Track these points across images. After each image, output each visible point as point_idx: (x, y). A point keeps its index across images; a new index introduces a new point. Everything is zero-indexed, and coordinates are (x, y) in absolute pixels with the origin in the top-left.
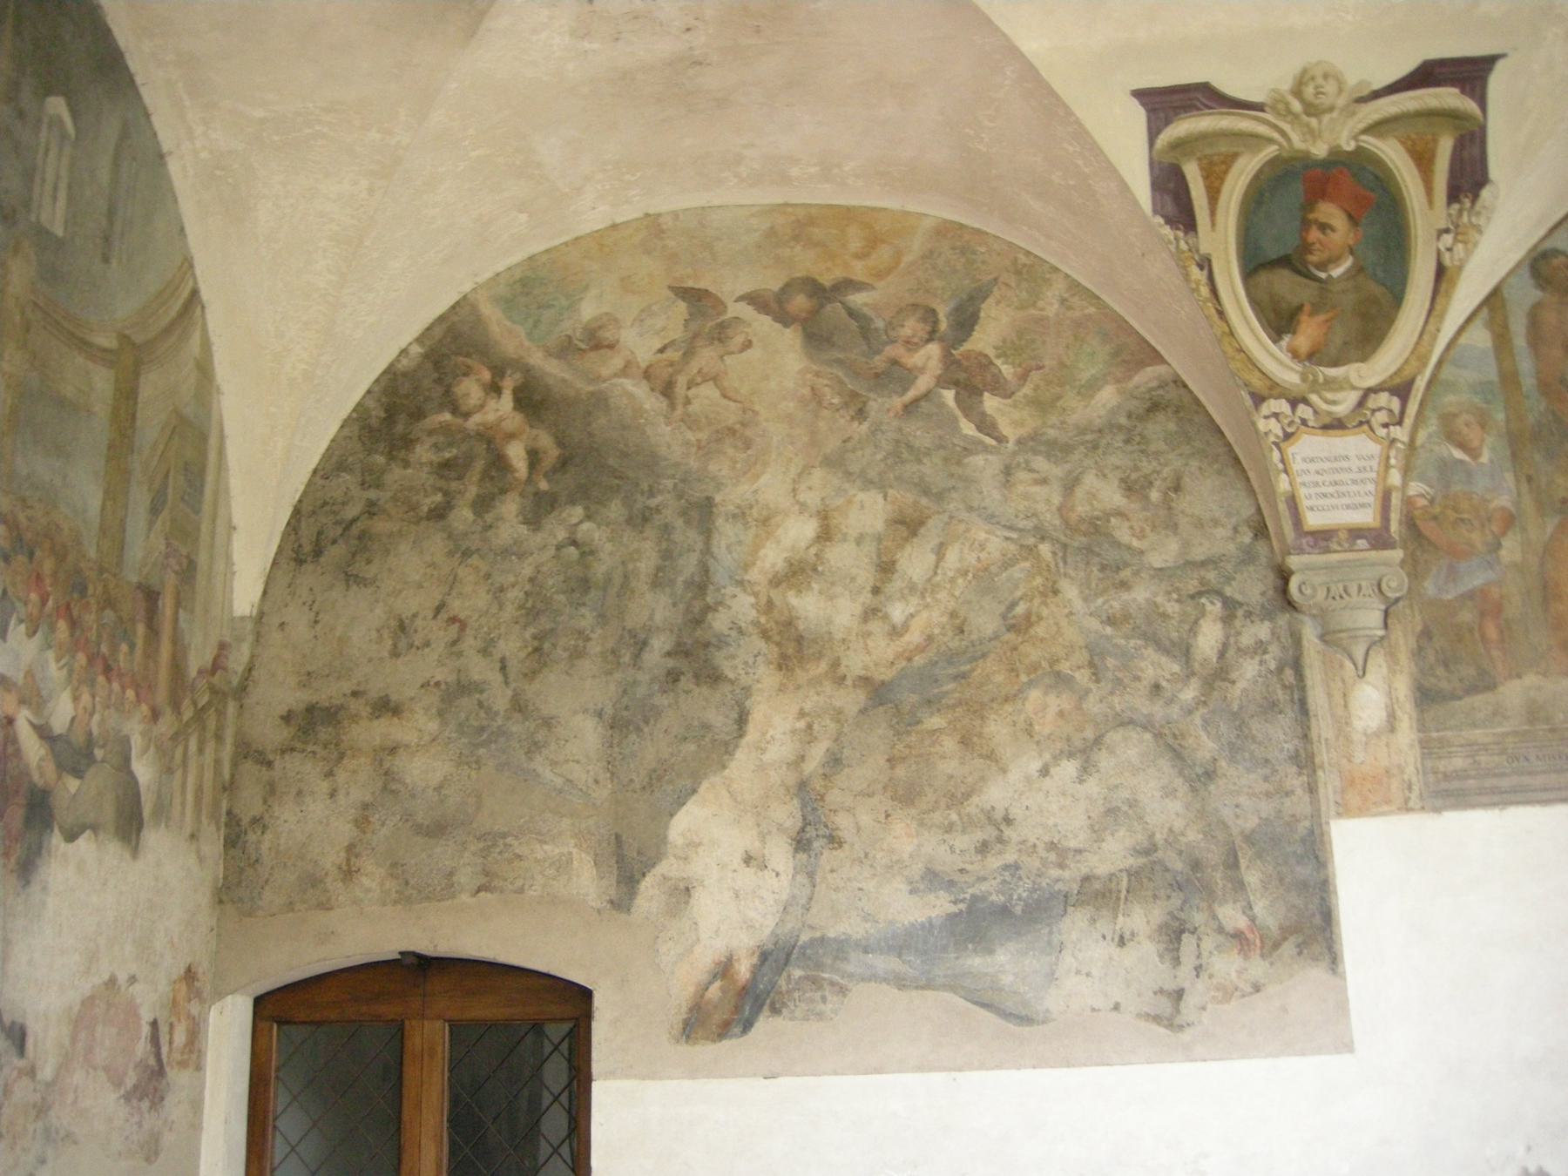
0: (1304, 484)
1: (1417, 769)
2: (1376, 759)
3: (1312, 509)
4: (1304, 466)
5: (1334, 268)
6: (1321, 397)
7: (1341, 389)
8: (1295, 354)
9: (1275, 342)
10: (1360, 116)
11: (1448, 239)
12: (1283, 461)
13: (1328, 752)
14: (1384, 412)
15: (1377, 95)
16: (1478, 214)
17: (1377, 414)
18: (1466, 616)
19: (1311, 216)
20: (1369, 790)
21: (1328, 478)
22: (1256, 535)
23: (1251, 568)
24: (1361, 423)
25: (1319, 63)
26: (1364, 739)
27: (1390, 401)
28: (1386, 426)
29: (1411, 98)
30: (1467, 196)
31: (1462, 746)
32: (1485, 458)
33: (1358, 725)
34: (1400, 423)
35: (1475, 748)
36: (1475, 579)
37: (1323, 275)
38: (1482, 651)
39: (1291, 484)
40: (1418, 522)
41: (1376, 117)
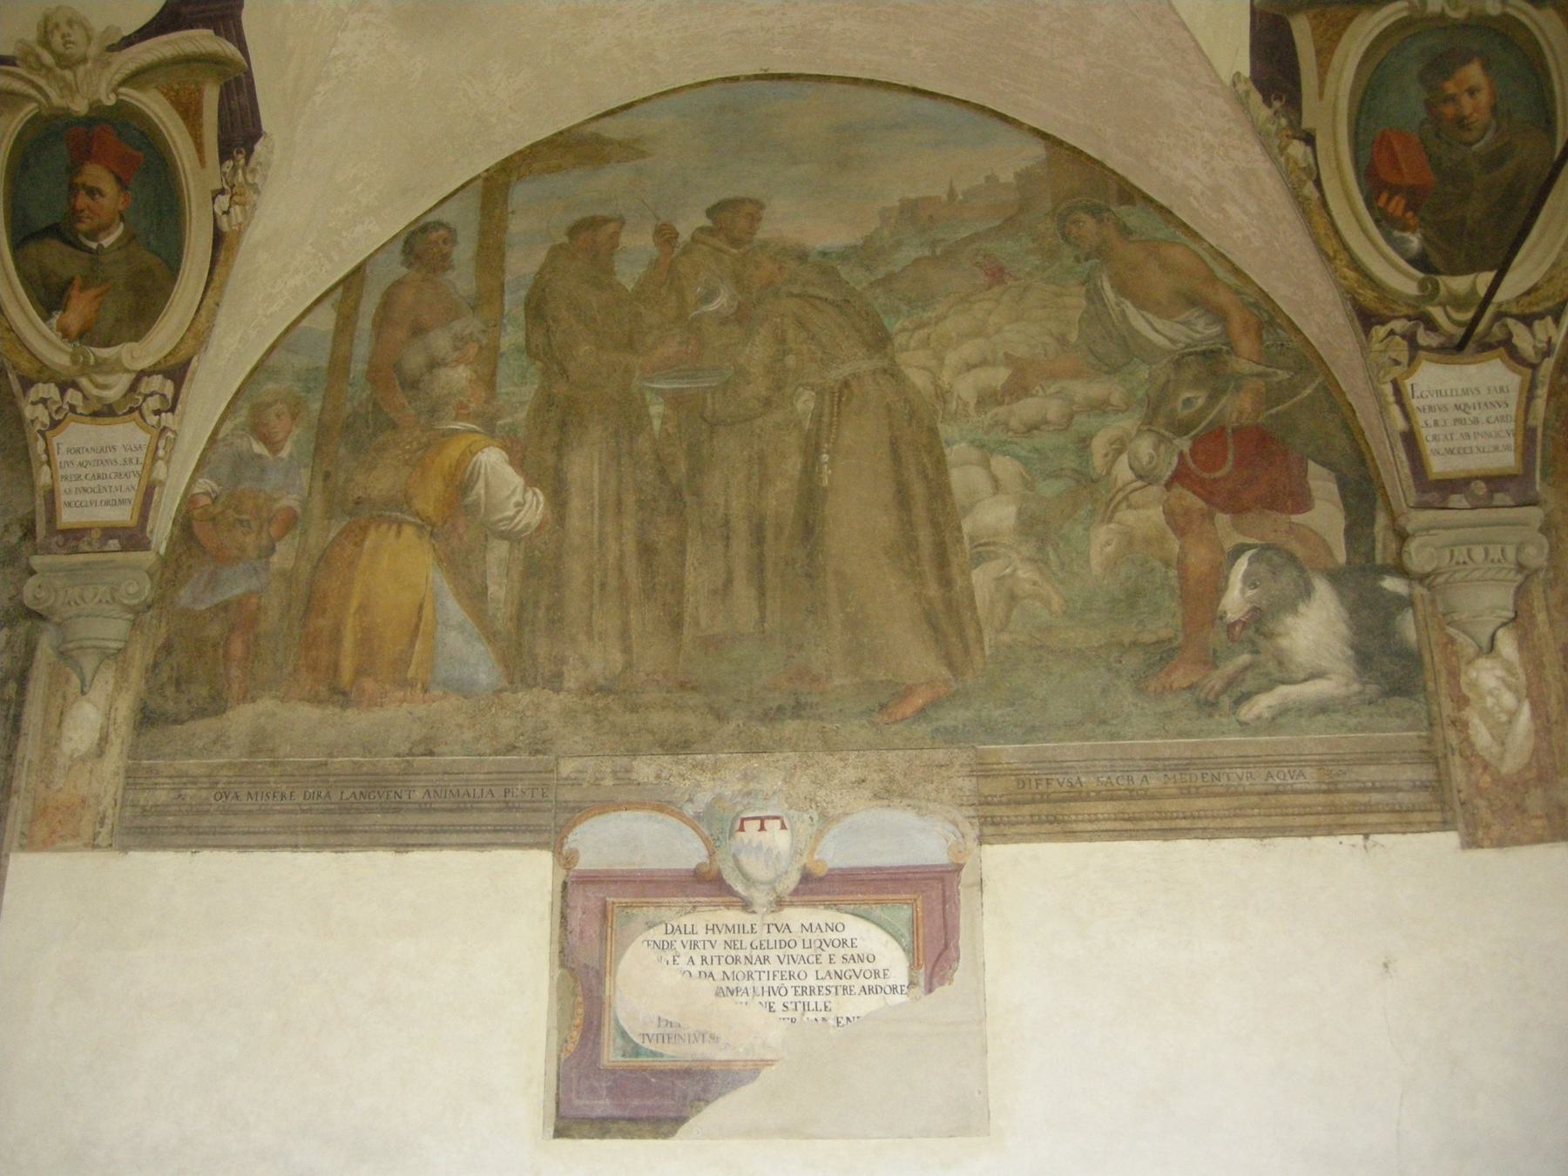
1: (115, 801)
2: (75, 787)
3: (70, 505)
4: (68, 457)
5: (105, 238)
6: (91, 381)
7: (112, 371)
8: (65, 334)
9: (45, 320)
10: (113, 68)
11: (223, 201)
12: (47, 451)
13: (28, 776)
14: (157, 397)
15: (128, 42)
16: (253, 171)
17: (149, 399)
18: (214, 630)
19: (79, 180)
20: (60, 822)
21: (90, 470)
22: (25, 535)
23: (8, 571)
24: (132, 410)
25: (58, 8)
28: (157, 412)
29: (166, 43)
30: (239, 152)
31: (171, 777)
32: (284, 454)
33: (67, 747)
34: (172, 410)
35: (184, 780)
36: (236, 586)
37: (94, 245)
38: (222, 671)
39: (52, 477)
40: (195, 524)
41: (132, 66)
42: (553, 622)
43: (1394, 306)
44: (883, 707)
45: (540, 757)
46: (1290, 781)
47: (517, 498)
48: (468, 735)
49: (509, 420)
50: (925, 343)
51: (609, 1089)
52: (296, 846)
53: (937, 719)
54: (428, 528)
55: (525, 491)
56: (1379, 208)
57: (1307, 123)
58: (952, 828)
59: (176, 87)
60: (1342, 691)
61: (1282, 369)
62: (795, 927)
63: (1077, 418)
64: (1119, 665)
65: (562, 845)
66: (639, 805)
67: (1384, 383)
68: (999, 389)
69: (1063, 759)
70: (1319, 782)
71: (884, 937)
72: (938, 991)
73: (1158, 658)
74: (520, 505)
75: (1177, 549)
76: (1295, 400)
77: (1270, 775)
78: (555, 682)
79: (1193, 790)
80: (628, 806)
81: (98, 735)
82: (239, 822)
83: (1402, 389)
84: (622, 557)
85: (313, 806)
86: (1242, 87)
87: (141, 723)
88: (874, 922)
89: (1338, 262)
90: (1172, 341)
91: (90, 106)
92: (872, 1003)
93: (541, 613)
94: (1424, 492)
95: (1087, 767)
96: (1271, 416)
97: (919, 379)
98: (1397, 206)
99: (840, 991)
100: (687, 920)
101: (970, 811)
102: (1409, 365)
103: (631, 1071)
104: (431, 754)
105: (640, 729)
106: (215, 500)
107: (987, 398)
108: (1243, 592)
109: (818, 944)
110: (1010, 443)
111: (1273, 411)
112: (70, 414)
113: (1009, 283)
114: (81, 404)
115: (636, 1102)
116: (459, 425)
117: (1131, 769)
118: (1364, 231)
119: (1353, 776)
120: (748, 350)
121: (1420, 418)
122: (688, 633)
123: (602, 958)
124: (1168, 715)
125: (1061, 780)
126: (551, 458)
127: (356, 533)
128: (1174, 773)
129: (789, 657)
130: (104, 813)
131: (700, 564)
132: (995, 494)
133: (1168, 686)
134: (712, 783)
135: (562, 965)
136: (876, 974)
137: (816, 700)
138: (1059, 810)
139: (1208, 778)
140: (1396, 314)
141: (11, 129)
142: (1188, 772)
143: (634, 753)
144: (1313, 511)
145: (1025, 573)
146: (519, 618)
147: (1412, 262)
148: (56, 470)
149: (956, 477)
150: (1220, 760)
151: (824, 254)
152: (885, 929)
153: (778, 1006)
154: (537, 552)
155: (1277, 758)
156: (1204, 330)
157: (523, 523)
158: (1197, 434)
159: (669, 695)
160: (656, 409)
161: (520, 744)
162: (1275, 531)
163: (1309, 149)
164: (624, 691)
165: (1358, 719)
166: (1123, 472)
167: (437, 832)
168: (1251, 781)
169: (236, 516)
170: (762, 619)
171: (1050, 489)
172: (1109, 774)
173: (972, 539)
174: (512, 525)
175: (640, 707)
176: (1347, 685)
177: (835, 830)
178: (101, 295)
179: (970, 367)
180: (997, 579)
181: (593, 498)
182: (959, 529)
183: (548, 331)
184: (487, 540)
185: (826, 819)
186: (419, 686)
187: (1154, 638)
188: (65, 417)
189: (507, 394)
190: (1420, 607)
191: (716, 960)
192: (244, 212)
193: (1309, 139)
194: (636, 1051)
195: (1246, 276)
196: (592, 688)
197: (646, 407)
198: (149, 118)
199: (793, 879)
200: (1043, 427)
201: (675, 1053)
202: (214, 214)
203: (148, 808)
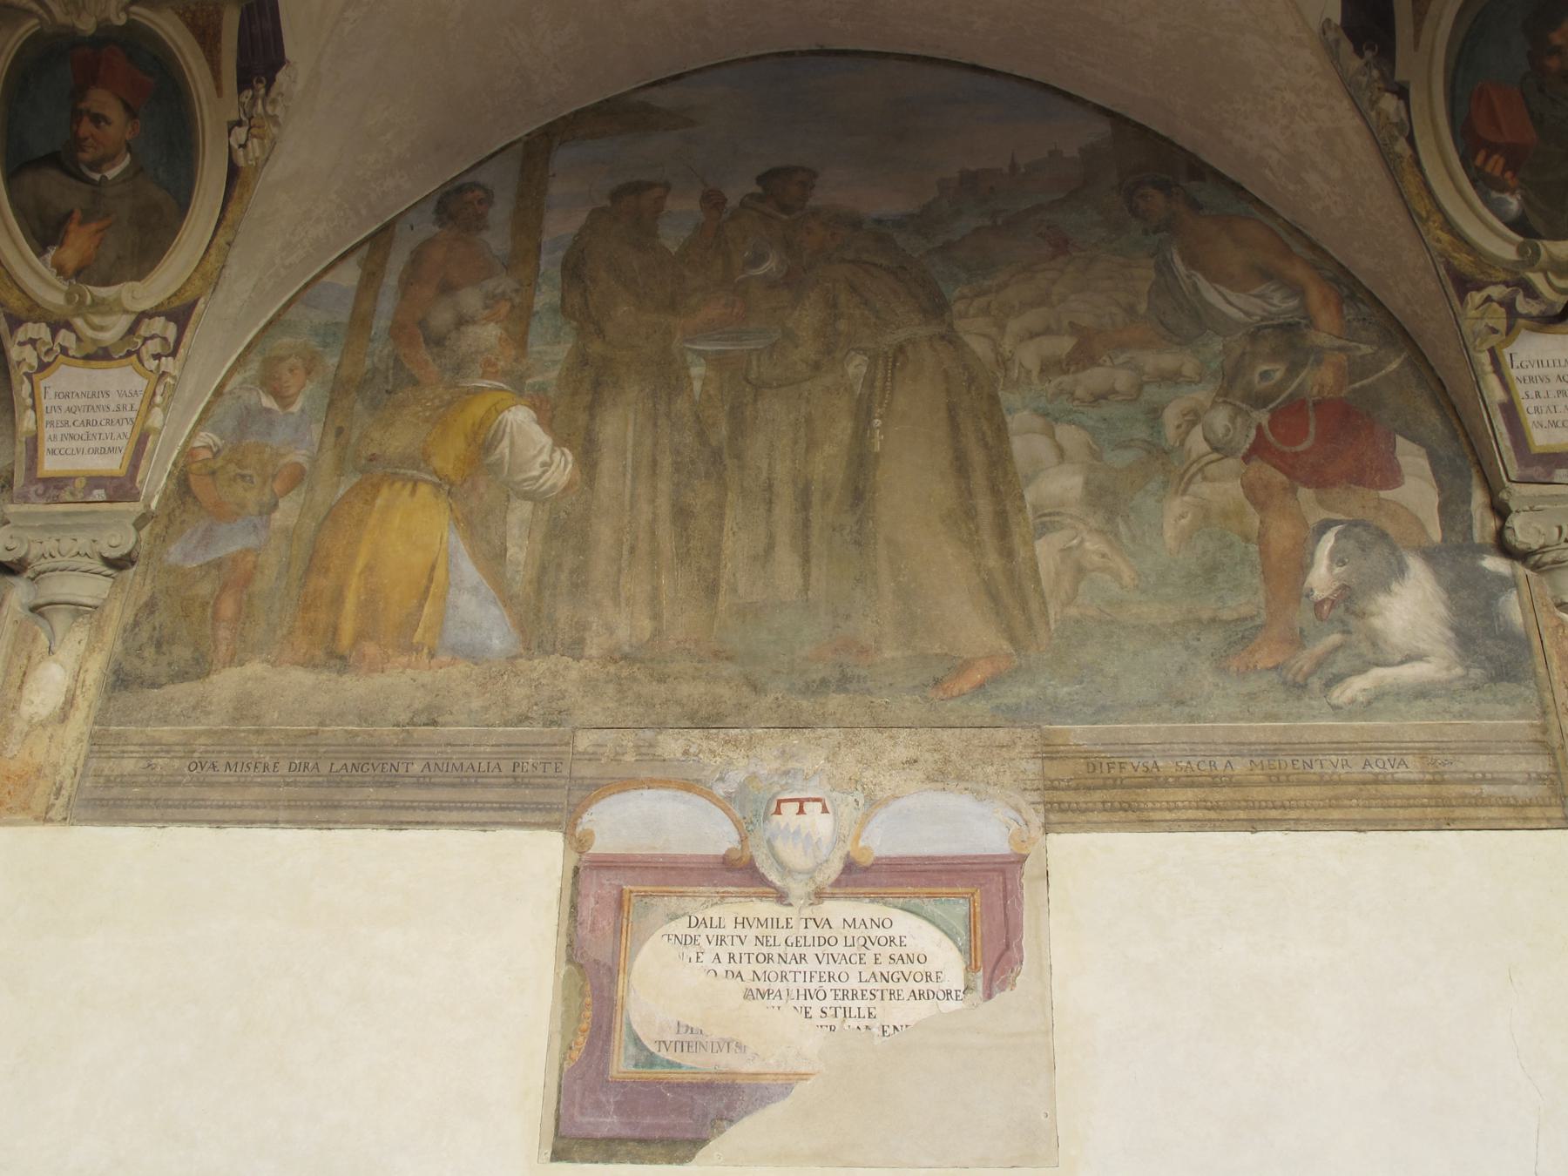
0: (51, 423)
3: (53, 452)
4: (57, 402)
5: (109, 169)
7: (110, 312)
8: (60, 270)
9: (39, 255)
11: (240, 134)
12: (32, 395)
14: (157, 340)
16: (274, 102)
17: (149, 342)
18: (205, 589)
19: (82, 106)
20: (9, 793)
24: (129, 354)
26: (26, 728)
27: (165, 328)
28: (157, 357)
30: (259, 81)
31: (141, 745)
32: (295, 408)
33: (26, 710)
34: (174, 354)
35: (157, 748)
36: (231, 543)
37: (97, 177)
38: (209, 632)
40: (192, 478)
42: (576, 586)
43: (1489, 271)
44: (937, 682)
45: (555, 728)
46: (1391, 770)
47: (545, 457)
48: (476, 704)
49: (539, 379)
50: (986, 311)
51: (619, 1104)
52: (276, 822)
53: (997, 697)
54: (446, 487)
55: (553, 451)
56: (1476, 167)
57: (1400, 76)
58: (1013, 814)
59: (193, 7)
60: (1443, 675)
61: (1365, 343)
62: (836, 922)
63: (1147, 388)
64: (1195, 643)
65: (575, 825)
66: (664, 783)
67: (1480, 352)
68: (1064, 357)
69: (1139, 741)
70: (1423, 772)
71: (938, 935)
72: (998, 996)
73: (1240, 636)
74: (546, 465)
75: (1257, 523)
76: (1380, 374)
77: (1367, 763)
78: (575, 648)
79: (1283, 778)
80: (651, 784)
81: (63, 698)
82: (215, 795)
83: (1501, 359)
84: (655, 520)
85: (298, 779)
86: (1331, 36)
87: (114, 687)
88: (925, 918)
89: (1431, 223)
90: (1247, 314)
91: (98, 24)
92: (923, 1008)
93: (564, 576)
94: (1527, 466)
95: (1164, 751)
96: (1355, 391)
97: (979, 347)
98: (1495, 165)
99: (887, 995)
100: (714, 913)
101: (1035, 797)
102: (1507, 334)
103: (644, 1084)
104: (434, 723)
105: (668, 700)
106: (215, 455)
107: (1049, 367)
108: (1330, 569)
109: (862, 941)
110: (1075, 412)
111: (1357, 385)
112: (61, 356)
113: (1074, 254)
114: (74, 346)
115: (648, 1120)
116: (485, 383)
117: (1213, 753)
118: (1460, 191)
119: (1461, 766)
120: (797, 314)
121: (1520, 389)
122: (724, 600)
123: (616, 954)
124: (1252, 696)
125: (1135, 764)
126: (582, 418)
127: (368, 490)
128: (1261, 758)
129: (834, 627)
130: (61, 783)
131: (740, 528)
132: (1060, 463)
133: (1251, 666)
134: (746, 760)
135: (570, 960)
136: (928, 977)
137: (864, 672)
138: (1134, 797)
139: (1299, 765)
140: (1493, 280)
141: (8, 47)
142: (1277, 758)
143: (661, 726)
144: (1403, 487)
145: (1093, 545)
146: (540, 581)
147: (1512, 225)
148: (42, 416)
149: (1018, 445)
150: (1312, 746)
151: (879, 221)
152: (938, 927)
153: (815, 1012)
154: (563, 514)
155: (1376, 745)
156: (1281, 304)
157: (549, 484)
158: (1277, 407)
159: (700, 665)
160: (698, 371)
161: (534, 715)
162: (1364, 507)
163: (1402, 104)
164: (652, 660)
165: (1463, 705)
166: (1197, 442)
167: (436, 809)
168: (1347, 769)
169: (239, 471)
170: (806, 587)
171: (1121, 459)
172: (1190, 759)
173: (1035, 509)
174: (538, 485)
175: (669, 677)
176: (1448, 669)
177: (882, 815)
178: (101, 230)
179: (1033, 336)
180: (1062, 550)
181: (626, 459)
182: (1022, 497)
183: (585, 291)
184: (509, 500)
185: (873, 803)
186: (426, 651)
187: (1235, 616)
188: (54, 360)
189: (539, 353)
190: (1524, 588)
191: (745, 958)
192: (262, 146)
193: (1402, 93)
194: (651, 1060)
195: (1324, 252)
196: (617, 656)
197: (688, 368)
198: (164, 42)
199: (836, 866)
200: (1111, 397)
201: (697, 1063)
202: (230, 146)
203: (112, 778)
